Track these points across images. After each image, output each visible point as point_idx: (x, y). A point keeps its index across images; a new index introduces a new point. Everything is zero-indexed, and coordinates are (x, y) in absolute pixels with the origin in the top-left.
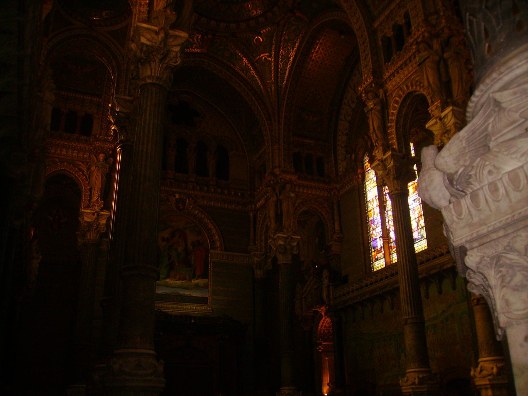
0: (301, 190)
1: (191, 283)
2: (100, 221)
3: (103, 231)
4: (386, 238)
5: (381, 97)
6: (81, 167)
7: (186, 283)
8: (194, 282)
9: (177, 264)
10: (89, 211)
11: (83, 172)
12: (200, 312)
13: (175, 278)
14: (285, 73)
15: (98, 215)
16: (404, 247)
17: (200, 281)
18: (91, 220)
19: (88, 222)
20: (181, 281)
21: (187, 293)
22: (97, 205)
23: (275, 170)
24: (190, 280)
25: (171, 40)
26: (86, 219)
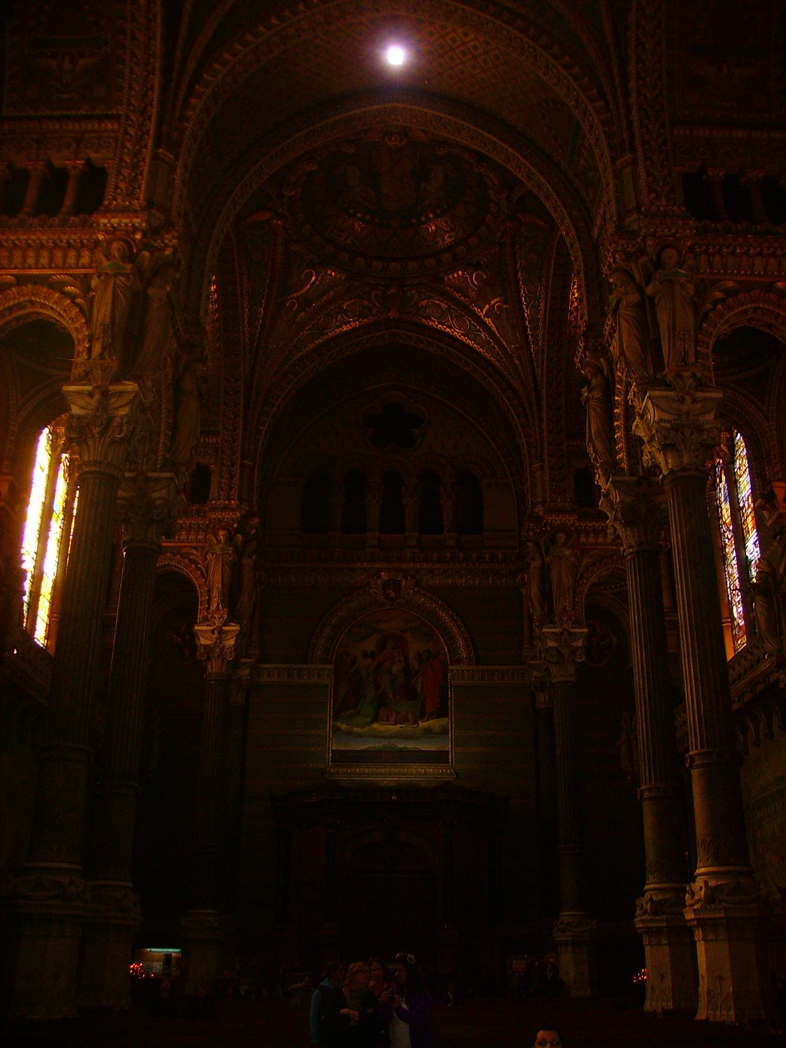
0: (591, 540)
1: (416, 727)
2: (224, 642)
3: (231, 657)
4: (726, 620)
5: (605, 373)
6: (192, 557)
7: (407, 728)
8: (423, 724)
9: (391, 696)
10: (205, 628)
11: (196, 563)
12: (432, 778)
13: (388, 720)
14: (538, 326)
15: (221, 632)
16: (641, 653)
17: (434, 723)
18: (211, 642)
19: (206, 646)
20: (400, 726)
21: (410, 745)
22: (216, 616)
23: (536, 510)
24: (416, 722)
25: (113, 400)
26: (203, 641)
